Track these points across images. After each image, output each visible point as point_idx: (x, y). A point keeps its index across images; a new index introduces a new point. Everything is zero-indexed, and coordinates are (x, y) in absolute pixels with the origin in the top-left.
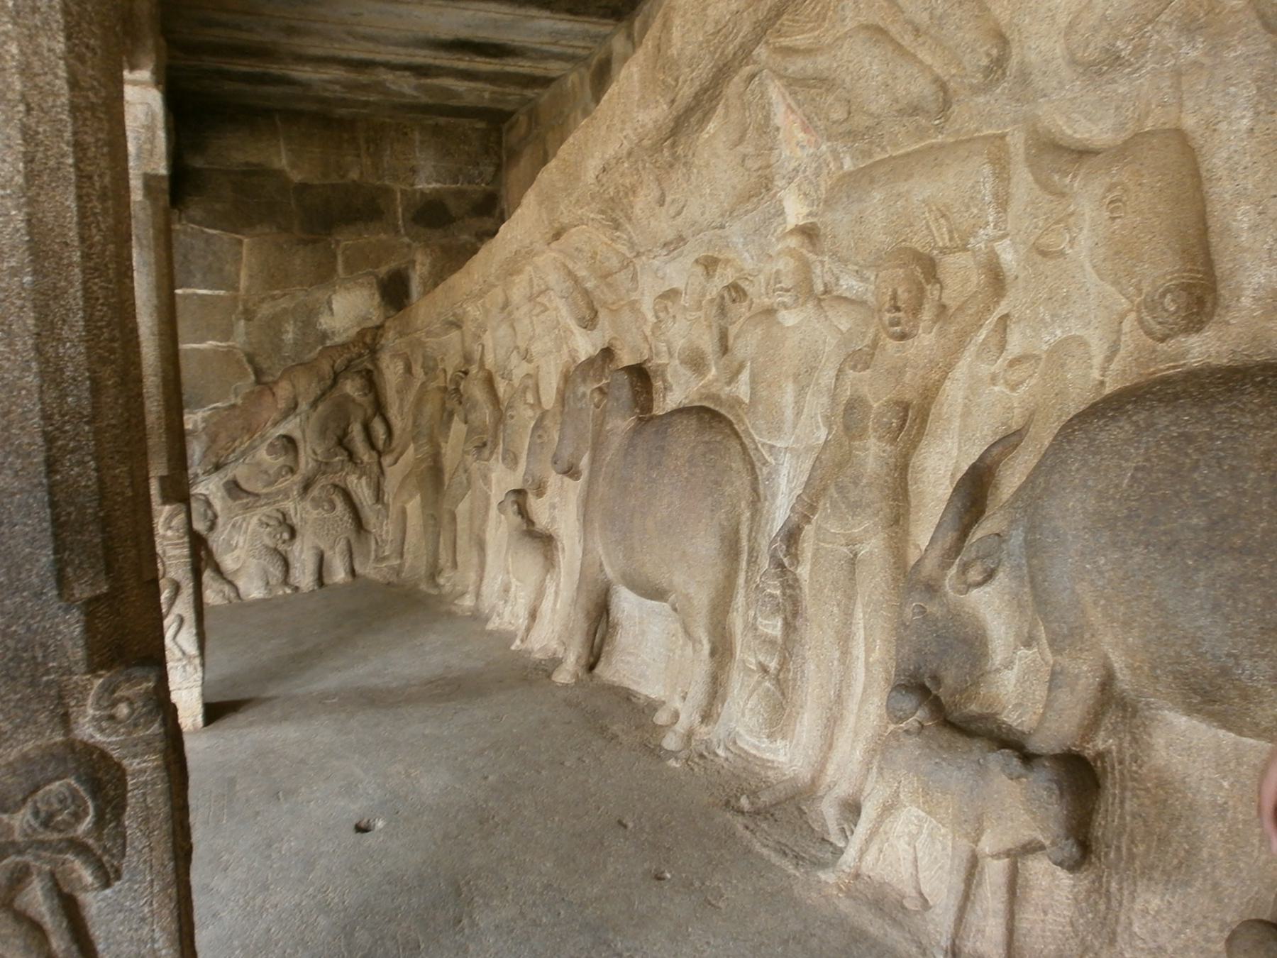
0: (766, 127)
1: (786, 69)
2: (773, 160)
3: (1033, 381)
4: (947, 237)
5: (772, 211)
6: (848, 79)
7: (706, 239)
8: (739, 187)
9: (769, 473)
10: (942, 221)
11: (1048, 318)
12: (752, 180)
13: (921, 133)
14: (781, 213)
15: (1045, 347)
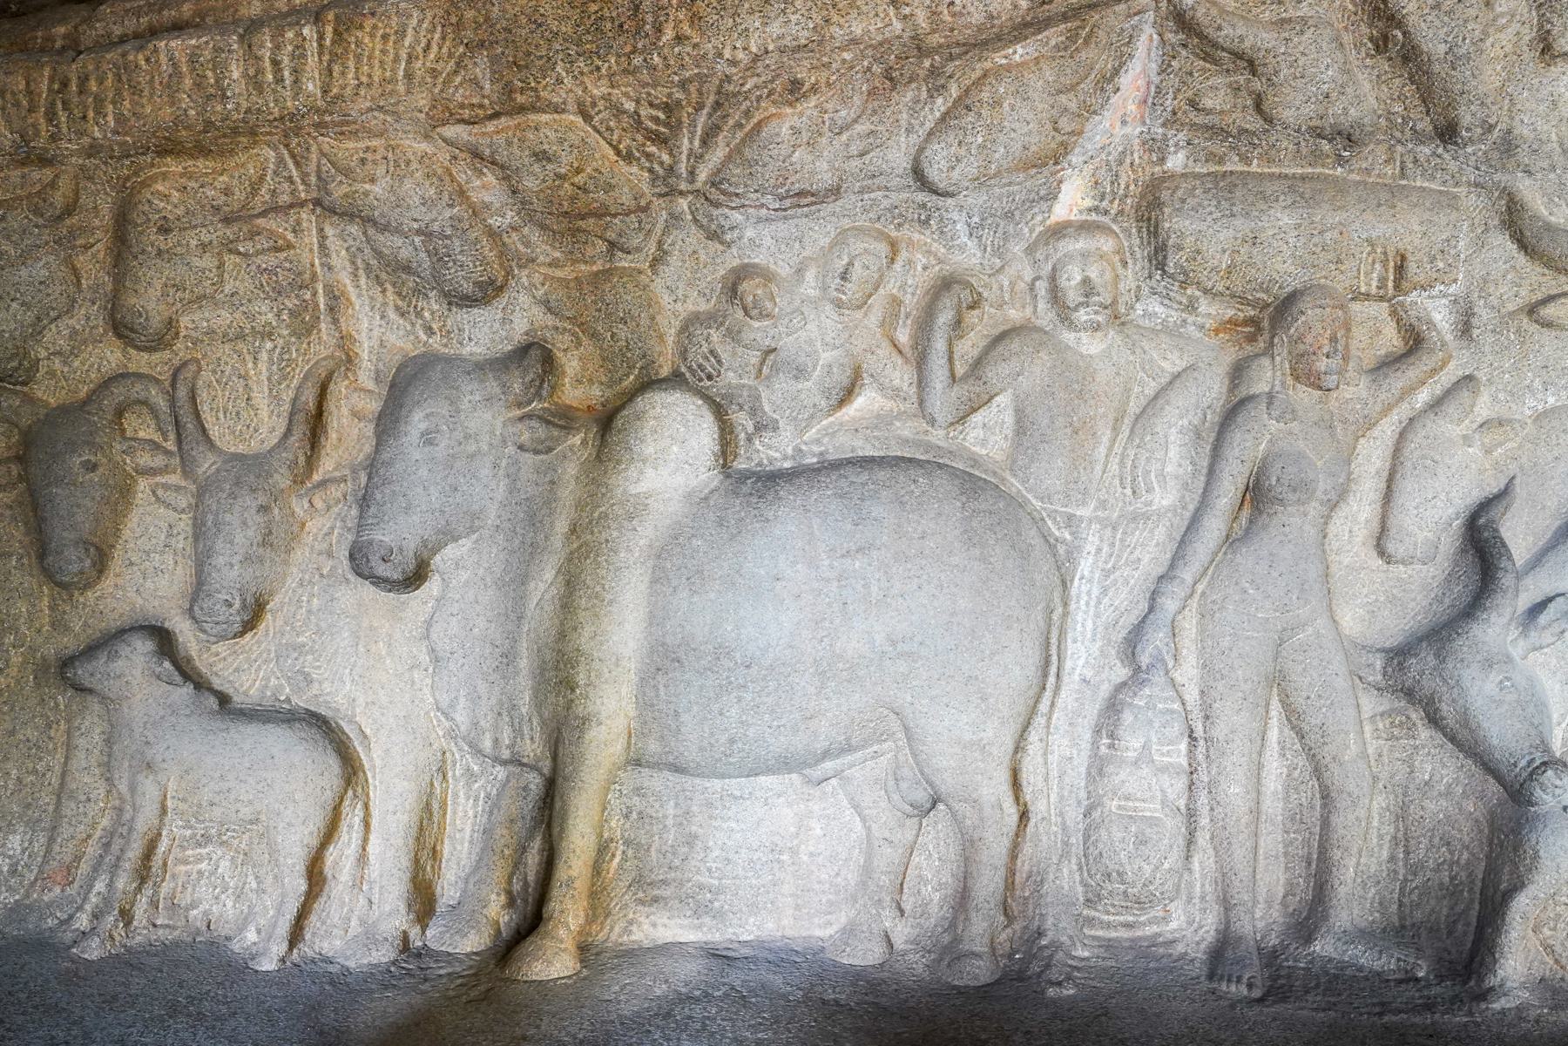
0: (1108, 81)
1: (1219, 28)
2: (1088, 127)
3: (1509, 445)
4: (1374, 284)
5: (1042, 193)
6: (1285, 72)
7: (886, 203)
8: (1033, 148)
9: (1068, 552)
10: (1378, 266)
11: (1537, 383)
12: (1053, 145)
13: (1316, 157)
14: (1052, 196)
15: (1529, 413)
